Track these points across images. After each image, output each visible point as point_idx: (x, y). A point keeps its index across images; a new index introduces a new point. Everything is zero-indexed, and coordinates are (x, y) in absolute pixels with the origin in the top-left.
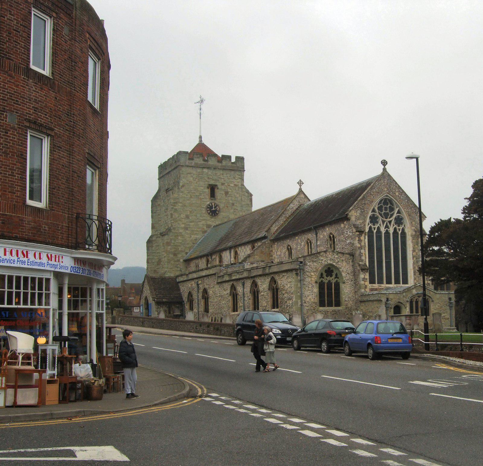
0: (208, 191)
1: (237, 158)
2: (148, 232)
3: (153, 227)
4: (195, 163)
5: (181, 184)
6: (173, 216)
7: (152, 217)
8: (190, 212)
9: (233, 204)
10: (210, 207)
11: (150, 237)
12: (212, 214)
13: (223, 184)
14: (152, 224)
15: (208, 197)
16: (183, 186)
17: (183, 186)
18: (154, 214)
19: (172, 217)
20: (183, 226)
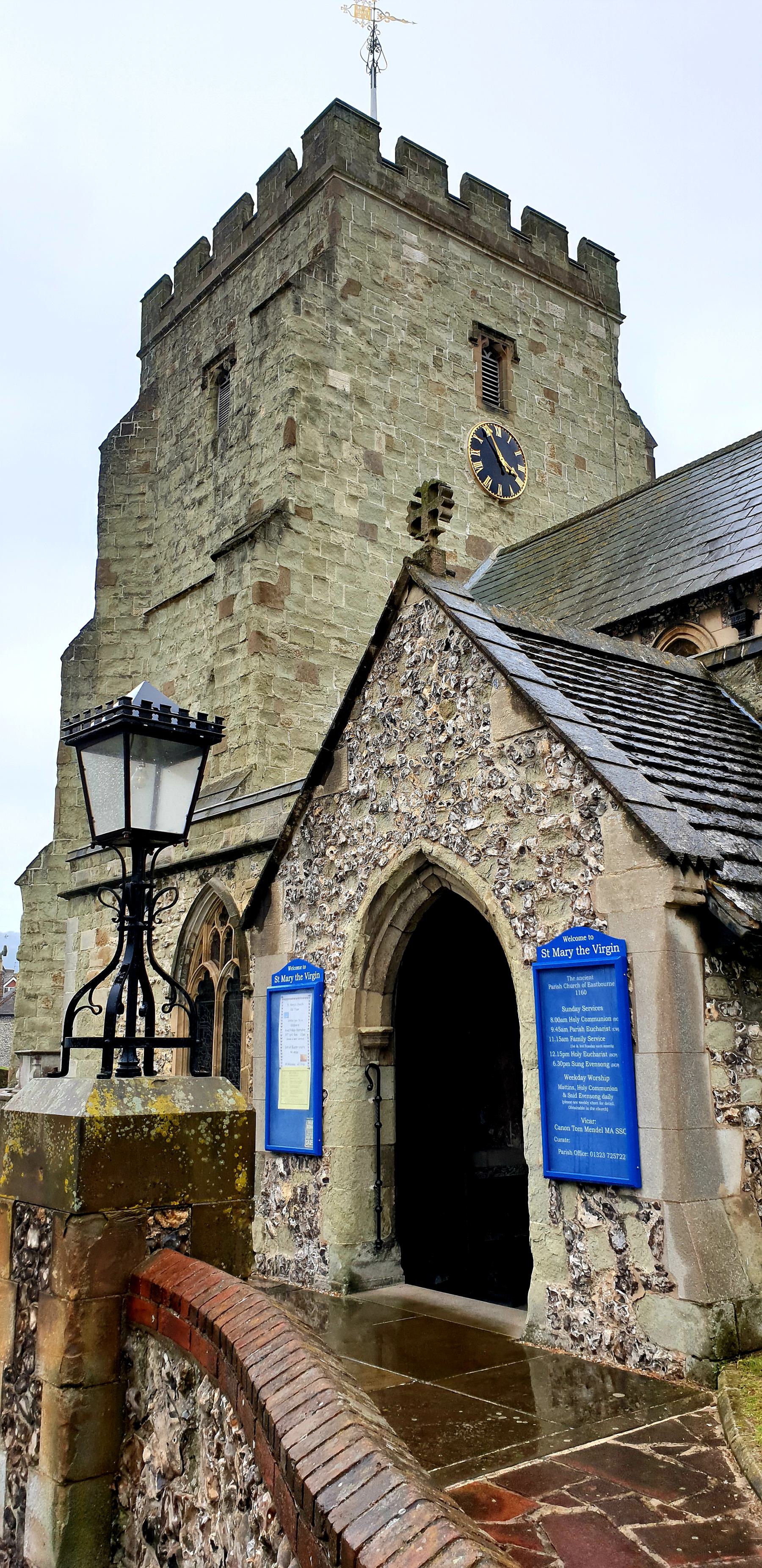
0: (472, 358)
1: (586, 245)
2: (78, 607)
3: (105, 578)
4: (414, 195)
5: (342, 275)
6: (300, 437)
7: (102, 526)
8: (390, 447)
9: (580, 463)
10: (484, 445)
11: (89, 627)
12: (494, 488)
13: (536, 348)
14: (102, 565)
15: (471, 390)
16: (353, 287)
17: (353, 287)
18: (117, 515)
19: (291, 442)
20: (352, 511)
